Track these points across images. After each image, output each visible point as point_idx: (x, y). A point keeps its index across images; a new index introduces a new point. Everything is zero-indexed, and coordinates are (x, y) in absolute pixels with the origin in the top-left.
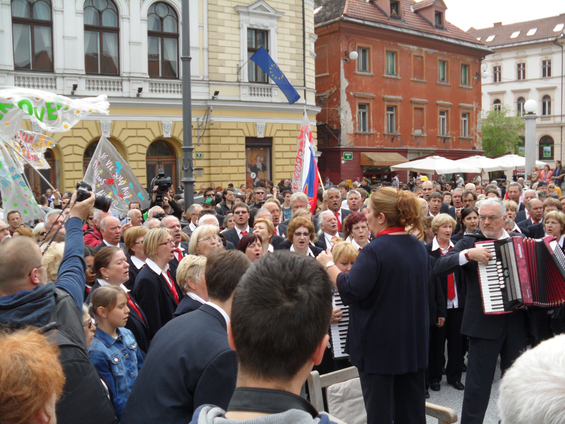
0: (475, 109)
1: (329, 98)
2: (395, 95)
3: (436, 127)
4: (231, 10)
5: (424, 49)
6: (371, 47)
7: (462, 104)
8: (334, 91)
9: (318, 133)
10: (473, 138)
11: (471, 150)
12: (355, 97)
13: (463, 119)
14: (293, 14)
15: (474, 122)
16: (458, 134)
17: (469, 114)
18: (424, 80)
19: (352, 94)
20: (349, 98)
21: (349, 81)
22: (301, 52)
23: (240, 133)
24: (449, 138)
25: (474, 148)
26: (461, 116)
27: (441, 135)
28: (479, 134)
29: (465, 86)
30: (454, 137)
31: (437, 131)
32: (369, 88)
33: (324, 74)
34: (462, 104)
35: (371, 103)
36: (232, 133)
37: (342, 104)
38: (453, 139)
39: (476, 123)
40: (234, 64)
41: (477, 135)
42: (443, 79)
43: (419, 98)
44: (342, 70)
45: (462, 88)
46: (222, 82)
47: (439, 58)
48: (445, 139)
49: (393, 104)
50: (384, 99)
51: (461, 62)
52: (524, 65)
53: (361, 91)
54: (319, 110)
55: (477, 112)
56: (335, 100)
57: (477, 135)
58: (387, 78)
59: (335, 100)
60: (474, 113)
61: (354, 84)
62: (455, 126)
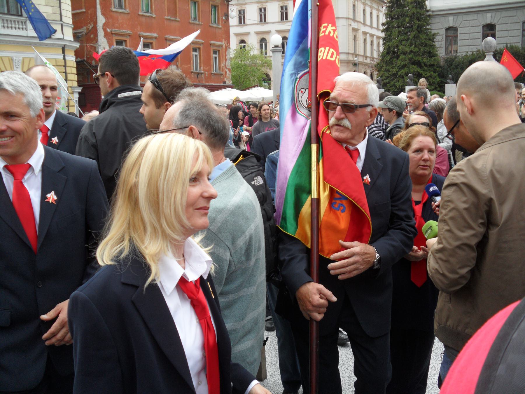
0: (224, 46)
1: (86, 34)
2: (150, 32)
3: (190, 63)
7: (212, 42)
8: (91, 27)
9: (77, 68)
10: (224, 73)
11: (222, 84)
12: (112, 33)
13: (214, 56)
15: (224, 58)
16: (210, 69)
17: (219, 51)
18: (178, 19)
19: (109, 30)
20: (106, 35)
21: (105, 18)
24: (201, 73)
25: (225, 82)
26: (212, 53)
27: (194, 71)
28: (229, 69)
29: (214, 25)
30: (207, 73)
31: (190, 67)
32: (125, 25)
33: (80, 11)
34: (212, 42)
35: (128, 39)
37: (99, 41)
38: (205, 74)
39: (226, 60)
41: (227, 70)
42: (195, 18)
43: (173, 36)
45: (212, 27)
48: (198, 74)
50: (140, 36)
51: (211, 3)
52: (265, 9)
53: (117, 28)
54: (77, 45)
55: (226, 50)
56: (92, 36)
57: (227, 70)
58: (143, 16)
59: (92, 36)
60: (224, 51)
61: (110, 21)
62: (207, 62)
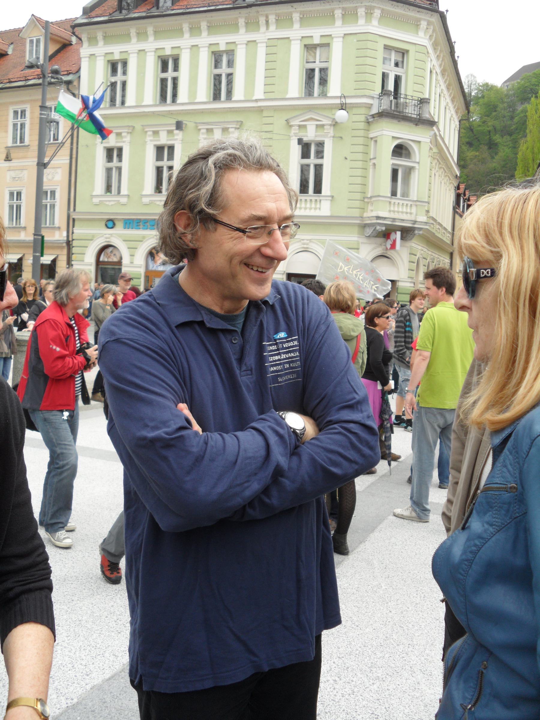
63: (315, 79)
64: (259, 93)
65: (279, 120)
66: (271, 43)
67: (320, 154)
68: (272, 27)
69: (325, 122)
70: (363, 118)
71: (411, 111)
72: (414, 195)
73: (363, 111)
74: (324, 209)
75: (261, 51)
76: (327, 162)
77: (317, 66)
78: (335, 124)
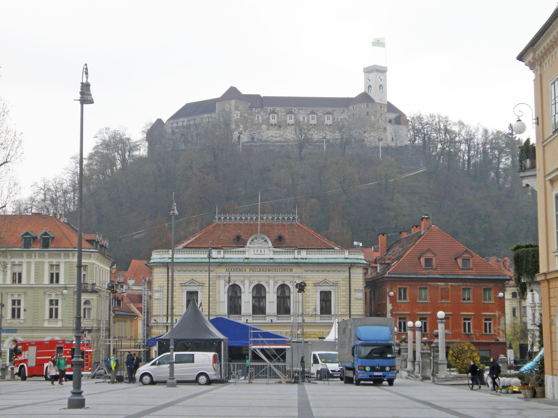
2: (427, 311)
4: (313, 285)
5: (450, 284)
6: (408, 287)
10: (497, 334)
11: (494, 341)
14: (344, 282)
20: (392, 315)
22: (348, 299)
23: (316, 336)
36: (312, 336)
40: (314, 307)
41: (501, 333)
44: (388, 301)
46: (307, 315)
47: (462, 287)
48: (468, 335)
49: (424, 317)
60: (497, 318)
63: (54, 278)
64: (32, 282)
65: (41, 292)
66: (37, 263)
67: (57, 304)
68: (37, 258)
69: (59, 293)
70: (72, 292)
71: (89, 288)
72: (92, 318)
73: (72, 289)
74: (60, 324)
75: (33, 267)
76: (60, 307)
77: (55, 272)
78: (62, 294)
